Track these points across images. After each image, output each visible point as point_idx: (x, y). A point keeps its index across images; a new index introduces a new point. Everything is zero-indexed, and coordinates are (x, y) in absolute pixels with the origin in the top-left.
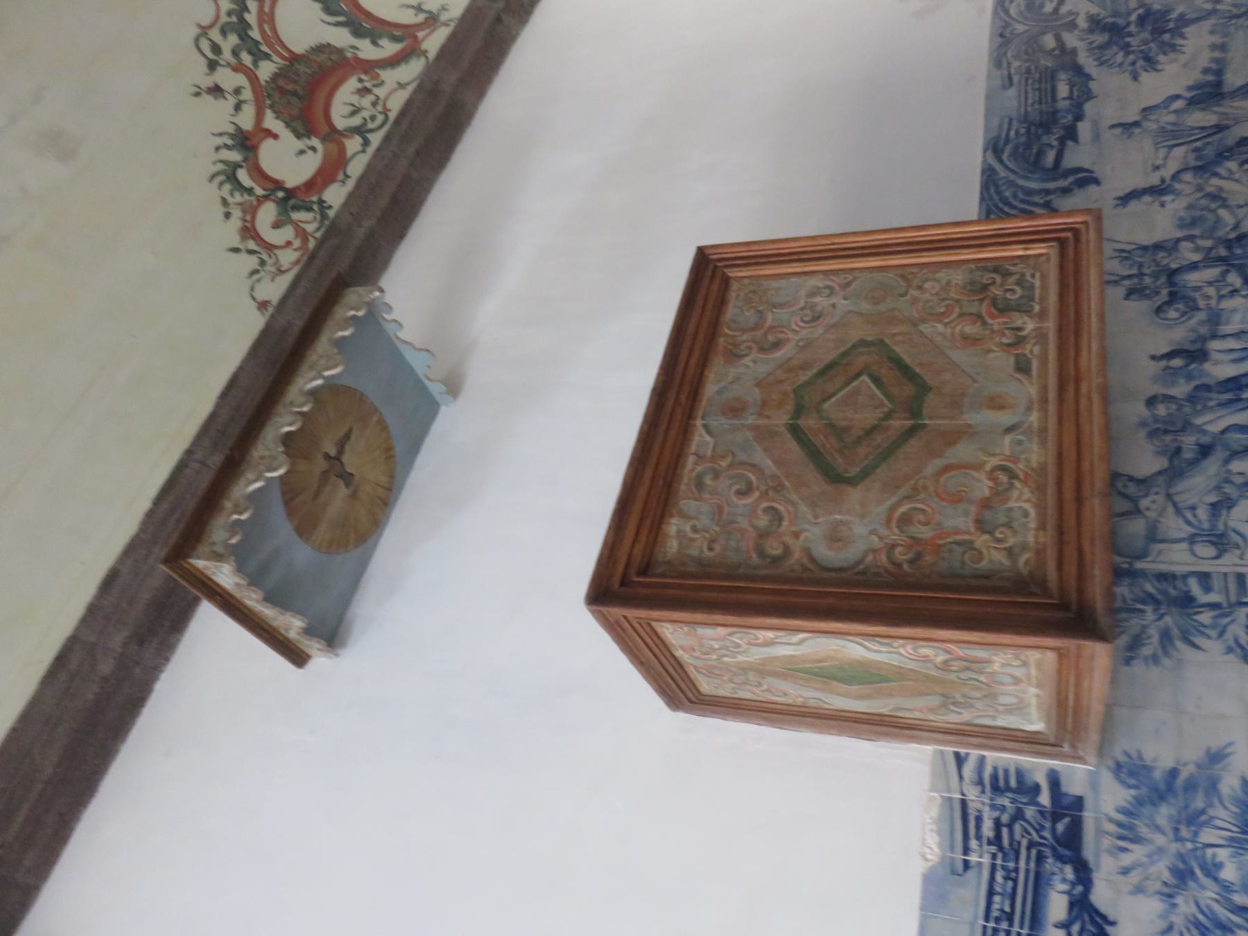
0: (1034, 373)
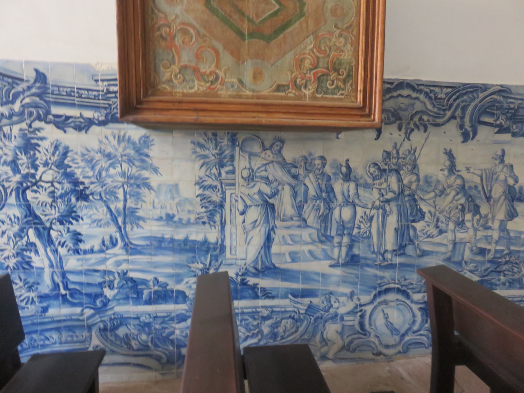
0: (276, 94)
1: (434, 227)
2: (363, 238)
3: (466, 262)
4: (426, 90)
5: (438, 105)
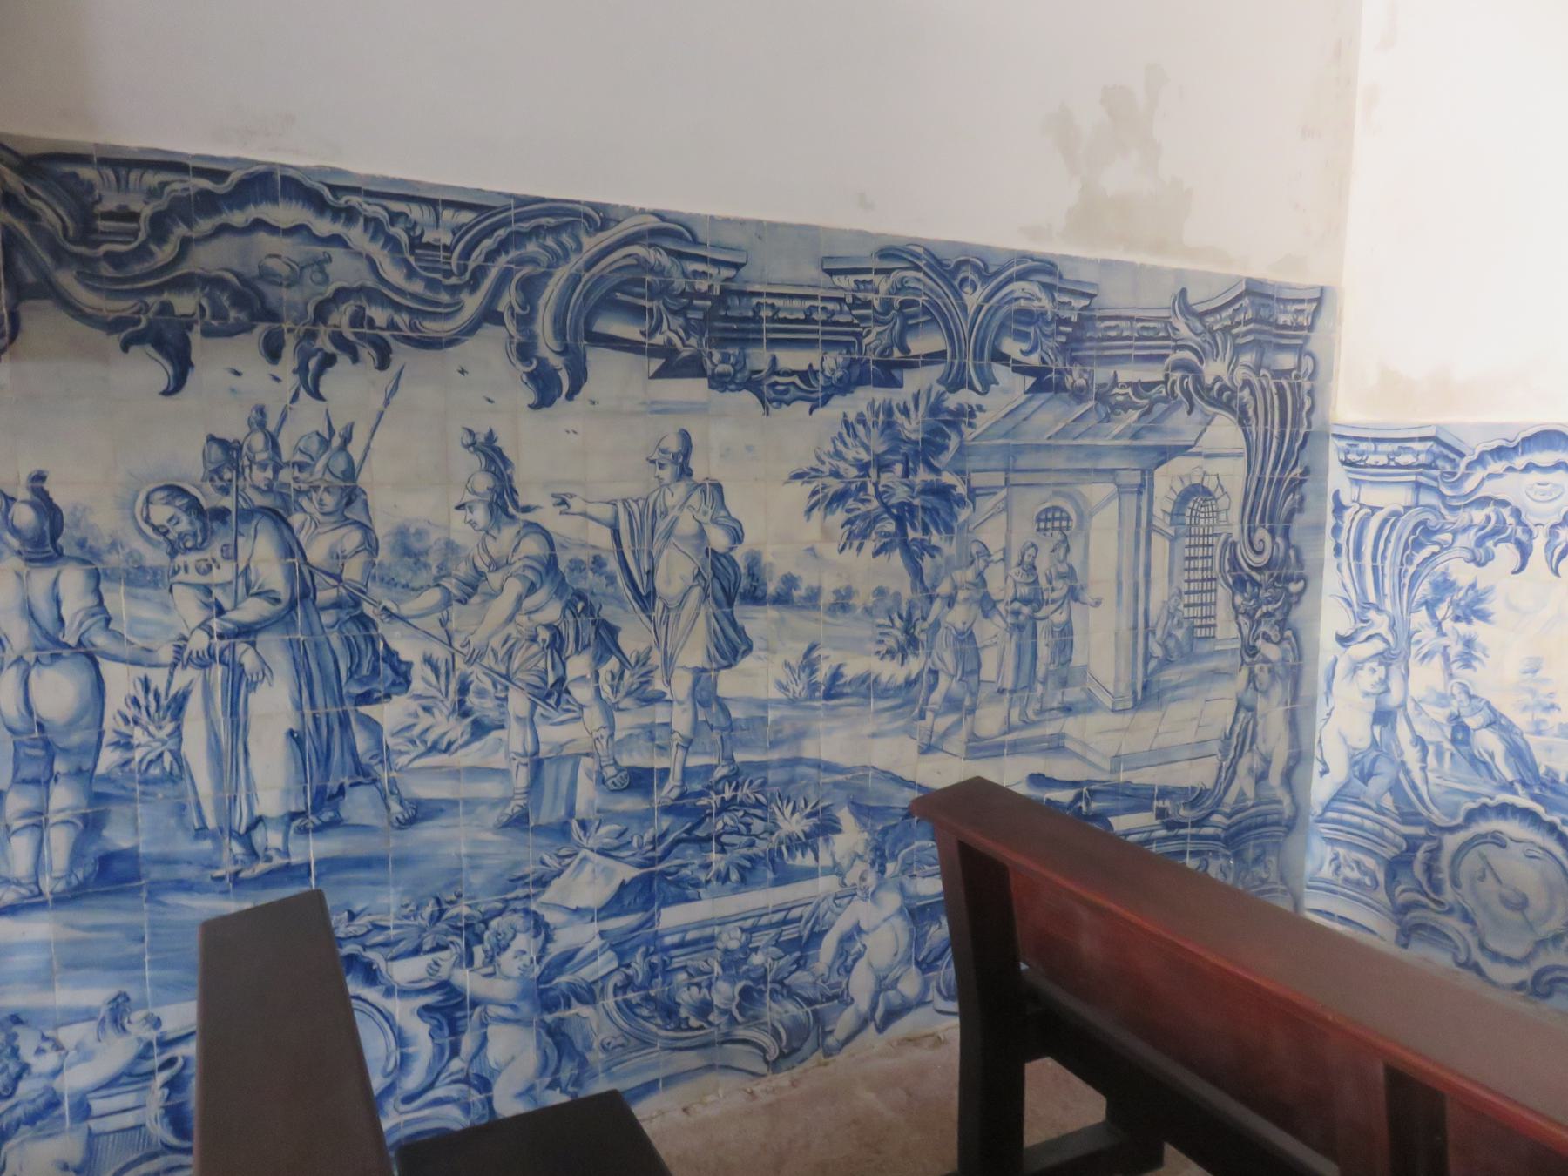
1: (454, 711)
2: (145, 782)
3: (583, 825)
4: (372, 209)
5: (426, 269)
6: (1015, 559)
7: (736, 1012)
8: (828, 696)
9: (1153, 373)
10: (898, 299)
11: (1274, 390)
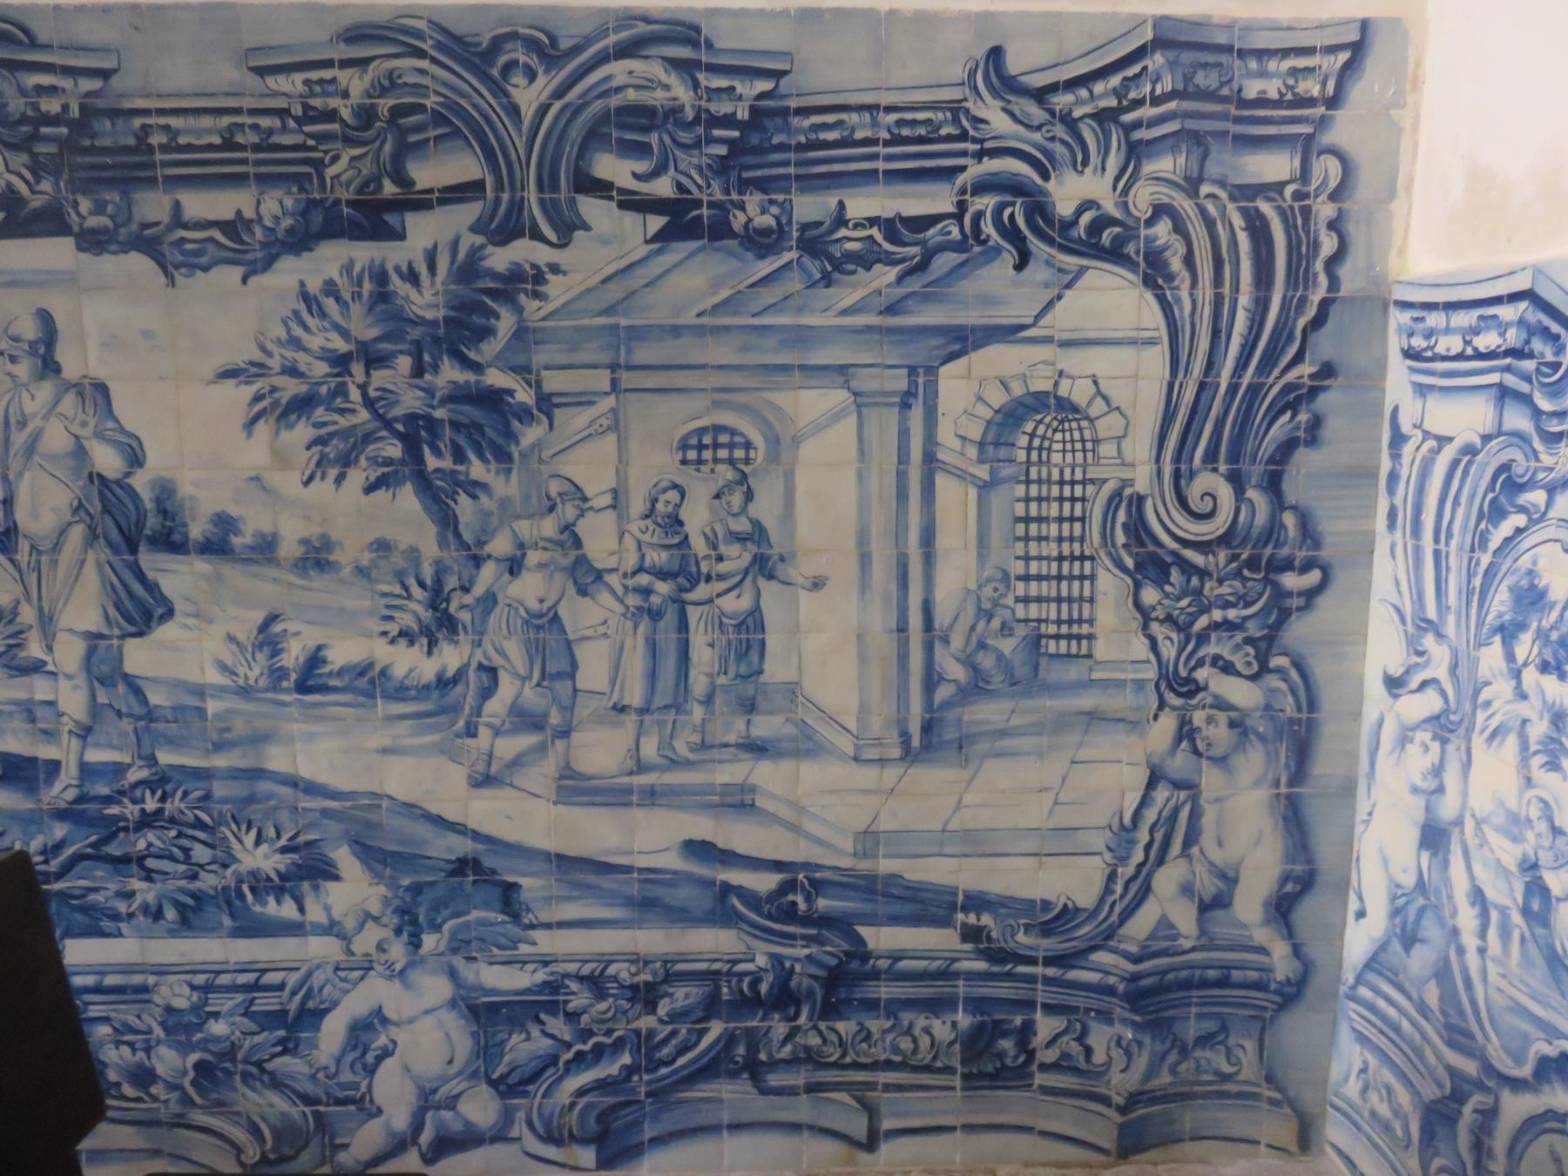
6: (638, 505)
7: (191, 1091)
8: (302, 687)
9: (934, 200)
10: (385, 104)
11: (1238, 221)
